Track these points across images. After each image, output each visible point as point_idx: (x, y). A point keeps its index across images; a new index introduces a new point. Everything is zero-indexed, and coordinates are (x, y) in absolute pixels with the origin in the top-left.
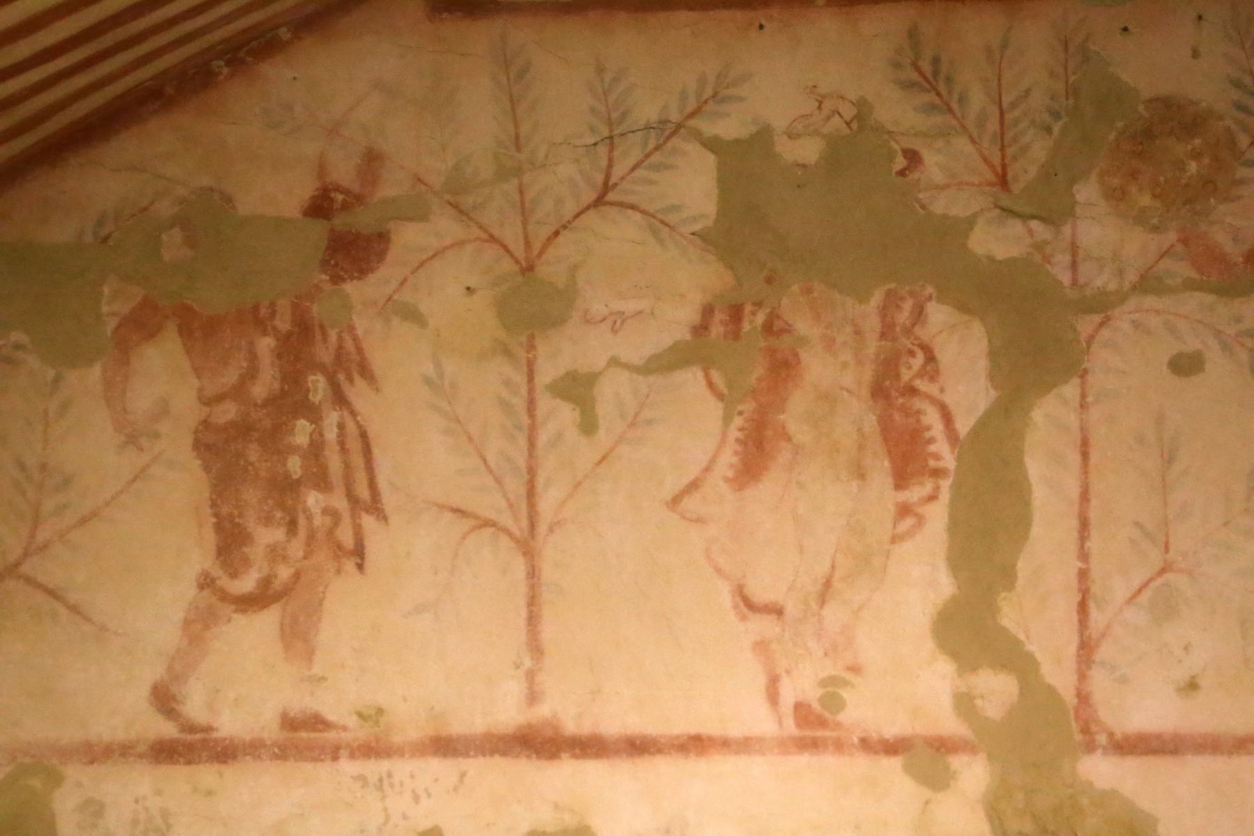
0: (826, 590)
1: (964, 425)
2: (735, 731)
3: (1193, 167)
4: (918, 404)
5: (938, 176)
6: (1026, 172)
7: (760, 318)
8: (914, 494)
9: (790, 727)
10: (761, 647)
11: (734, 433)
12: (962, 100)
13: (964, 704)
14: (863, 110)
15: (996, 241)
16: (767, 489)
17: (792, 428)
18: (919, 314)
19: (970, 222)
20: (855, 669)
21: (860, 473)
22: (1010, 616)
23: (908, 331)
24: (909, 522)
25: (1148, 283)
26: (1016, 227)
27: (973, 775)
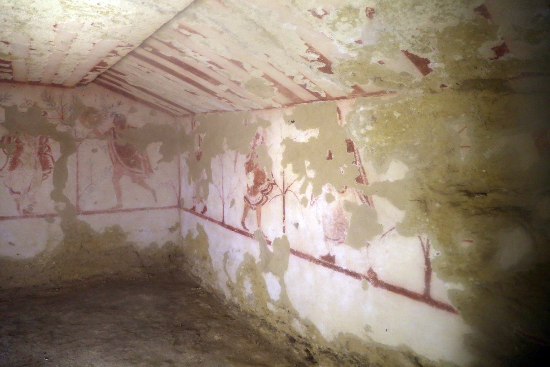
0: (29, 189)
1: (56, 160)
2: (10, 215)
3: (95, 119)
4: (47, 156)
5: (50, 117)
6: (67, 117)
7: (15, 140)
8: (47, 171)
9: (22, 214)
10: (16, 200)
11: (9, 161)
12: (55, 104)
13: (56, 208)
14: (35, 105)
15: (61, 128)
16: (16, 171)
17: (22, 160)
18: (47, 140)
19: (57, 125)
20: (35, 203)
21: (35, 168)
22: (64, 192)
23: (45, 143)
24: (45, 177)
25: (88, 137)
26: (65, 126)
27: (58, 220)
